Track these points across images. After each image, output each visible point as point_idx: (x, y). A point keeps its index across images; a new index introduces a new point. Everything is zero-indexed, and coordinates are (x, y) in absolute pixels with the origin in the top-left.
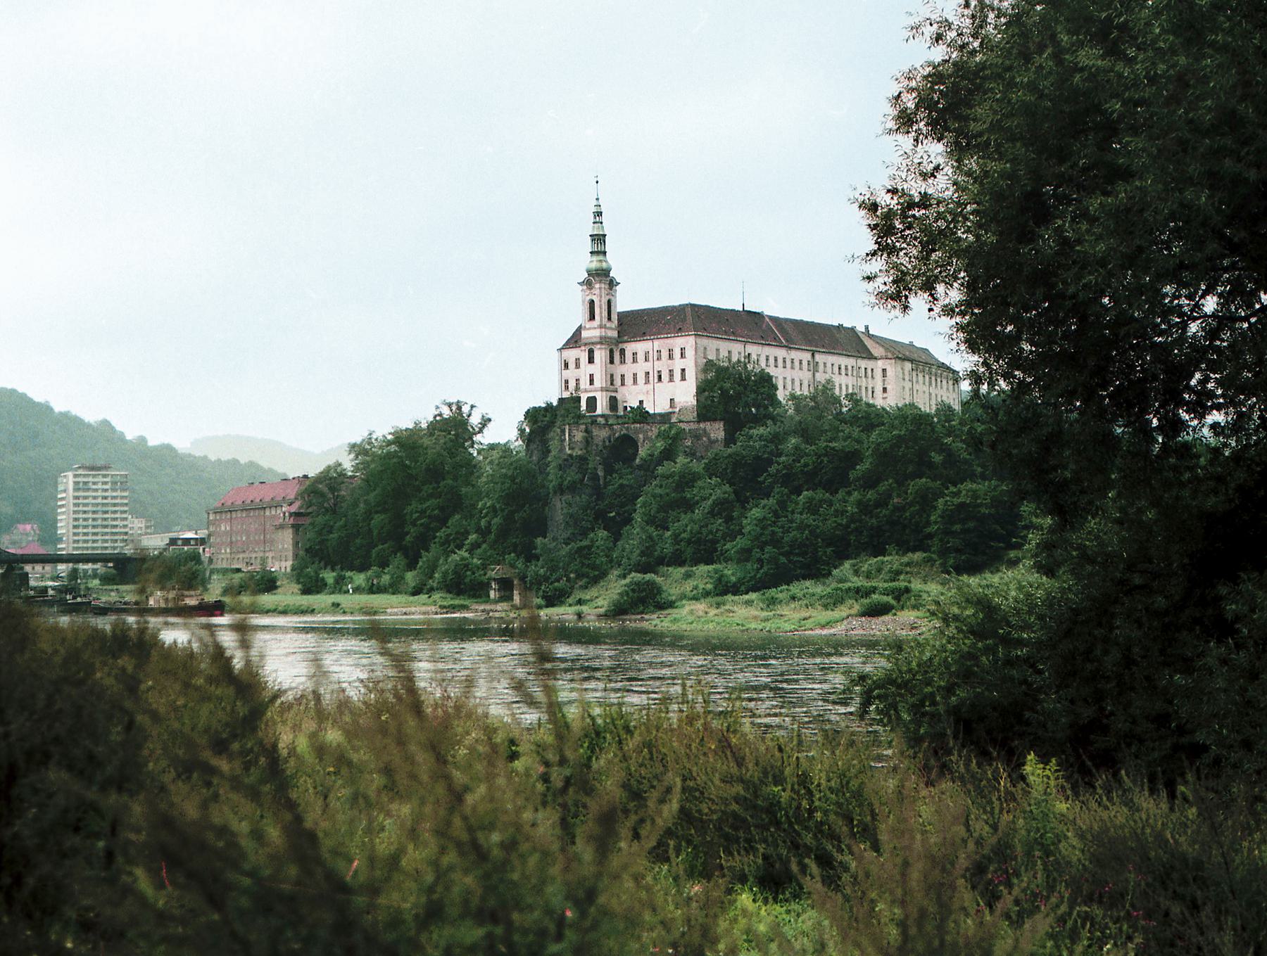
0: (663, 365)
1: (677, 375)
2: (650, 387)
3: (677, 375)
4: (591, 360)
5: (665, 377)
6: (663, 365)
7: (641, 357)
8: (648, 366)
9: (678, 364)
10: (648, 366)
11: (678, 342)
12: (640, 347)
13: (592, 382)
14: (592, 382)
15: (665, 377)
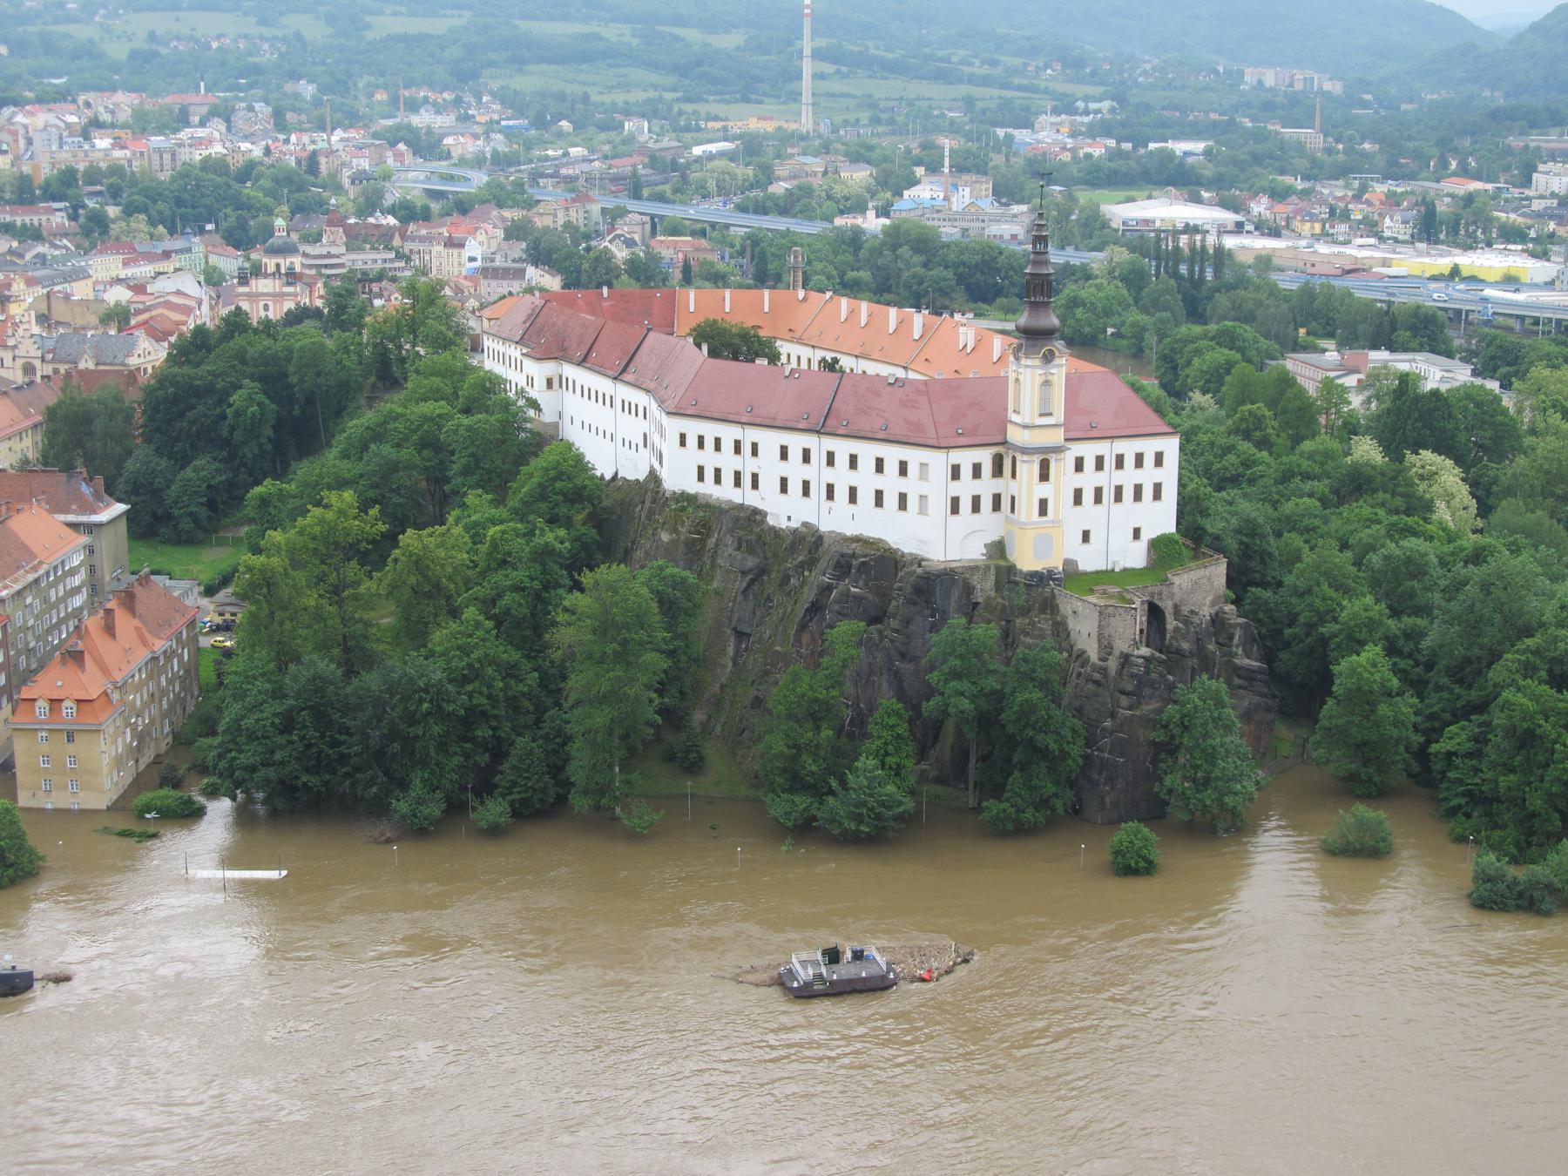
0: (1128, 477)
1: (1148, 492)
2: (1101, 509)
3: (1148, 492)
4: (1044, 476)
5: (1128, 494)
6: (1128, 477)
7: (1089, 464)
8: (1101, 479)
10: (1101, 479)
11: (1149, 447)
12: (1089, 451)
13: (1043, 510)
14: (1043, 510)
15: (1128, 494)
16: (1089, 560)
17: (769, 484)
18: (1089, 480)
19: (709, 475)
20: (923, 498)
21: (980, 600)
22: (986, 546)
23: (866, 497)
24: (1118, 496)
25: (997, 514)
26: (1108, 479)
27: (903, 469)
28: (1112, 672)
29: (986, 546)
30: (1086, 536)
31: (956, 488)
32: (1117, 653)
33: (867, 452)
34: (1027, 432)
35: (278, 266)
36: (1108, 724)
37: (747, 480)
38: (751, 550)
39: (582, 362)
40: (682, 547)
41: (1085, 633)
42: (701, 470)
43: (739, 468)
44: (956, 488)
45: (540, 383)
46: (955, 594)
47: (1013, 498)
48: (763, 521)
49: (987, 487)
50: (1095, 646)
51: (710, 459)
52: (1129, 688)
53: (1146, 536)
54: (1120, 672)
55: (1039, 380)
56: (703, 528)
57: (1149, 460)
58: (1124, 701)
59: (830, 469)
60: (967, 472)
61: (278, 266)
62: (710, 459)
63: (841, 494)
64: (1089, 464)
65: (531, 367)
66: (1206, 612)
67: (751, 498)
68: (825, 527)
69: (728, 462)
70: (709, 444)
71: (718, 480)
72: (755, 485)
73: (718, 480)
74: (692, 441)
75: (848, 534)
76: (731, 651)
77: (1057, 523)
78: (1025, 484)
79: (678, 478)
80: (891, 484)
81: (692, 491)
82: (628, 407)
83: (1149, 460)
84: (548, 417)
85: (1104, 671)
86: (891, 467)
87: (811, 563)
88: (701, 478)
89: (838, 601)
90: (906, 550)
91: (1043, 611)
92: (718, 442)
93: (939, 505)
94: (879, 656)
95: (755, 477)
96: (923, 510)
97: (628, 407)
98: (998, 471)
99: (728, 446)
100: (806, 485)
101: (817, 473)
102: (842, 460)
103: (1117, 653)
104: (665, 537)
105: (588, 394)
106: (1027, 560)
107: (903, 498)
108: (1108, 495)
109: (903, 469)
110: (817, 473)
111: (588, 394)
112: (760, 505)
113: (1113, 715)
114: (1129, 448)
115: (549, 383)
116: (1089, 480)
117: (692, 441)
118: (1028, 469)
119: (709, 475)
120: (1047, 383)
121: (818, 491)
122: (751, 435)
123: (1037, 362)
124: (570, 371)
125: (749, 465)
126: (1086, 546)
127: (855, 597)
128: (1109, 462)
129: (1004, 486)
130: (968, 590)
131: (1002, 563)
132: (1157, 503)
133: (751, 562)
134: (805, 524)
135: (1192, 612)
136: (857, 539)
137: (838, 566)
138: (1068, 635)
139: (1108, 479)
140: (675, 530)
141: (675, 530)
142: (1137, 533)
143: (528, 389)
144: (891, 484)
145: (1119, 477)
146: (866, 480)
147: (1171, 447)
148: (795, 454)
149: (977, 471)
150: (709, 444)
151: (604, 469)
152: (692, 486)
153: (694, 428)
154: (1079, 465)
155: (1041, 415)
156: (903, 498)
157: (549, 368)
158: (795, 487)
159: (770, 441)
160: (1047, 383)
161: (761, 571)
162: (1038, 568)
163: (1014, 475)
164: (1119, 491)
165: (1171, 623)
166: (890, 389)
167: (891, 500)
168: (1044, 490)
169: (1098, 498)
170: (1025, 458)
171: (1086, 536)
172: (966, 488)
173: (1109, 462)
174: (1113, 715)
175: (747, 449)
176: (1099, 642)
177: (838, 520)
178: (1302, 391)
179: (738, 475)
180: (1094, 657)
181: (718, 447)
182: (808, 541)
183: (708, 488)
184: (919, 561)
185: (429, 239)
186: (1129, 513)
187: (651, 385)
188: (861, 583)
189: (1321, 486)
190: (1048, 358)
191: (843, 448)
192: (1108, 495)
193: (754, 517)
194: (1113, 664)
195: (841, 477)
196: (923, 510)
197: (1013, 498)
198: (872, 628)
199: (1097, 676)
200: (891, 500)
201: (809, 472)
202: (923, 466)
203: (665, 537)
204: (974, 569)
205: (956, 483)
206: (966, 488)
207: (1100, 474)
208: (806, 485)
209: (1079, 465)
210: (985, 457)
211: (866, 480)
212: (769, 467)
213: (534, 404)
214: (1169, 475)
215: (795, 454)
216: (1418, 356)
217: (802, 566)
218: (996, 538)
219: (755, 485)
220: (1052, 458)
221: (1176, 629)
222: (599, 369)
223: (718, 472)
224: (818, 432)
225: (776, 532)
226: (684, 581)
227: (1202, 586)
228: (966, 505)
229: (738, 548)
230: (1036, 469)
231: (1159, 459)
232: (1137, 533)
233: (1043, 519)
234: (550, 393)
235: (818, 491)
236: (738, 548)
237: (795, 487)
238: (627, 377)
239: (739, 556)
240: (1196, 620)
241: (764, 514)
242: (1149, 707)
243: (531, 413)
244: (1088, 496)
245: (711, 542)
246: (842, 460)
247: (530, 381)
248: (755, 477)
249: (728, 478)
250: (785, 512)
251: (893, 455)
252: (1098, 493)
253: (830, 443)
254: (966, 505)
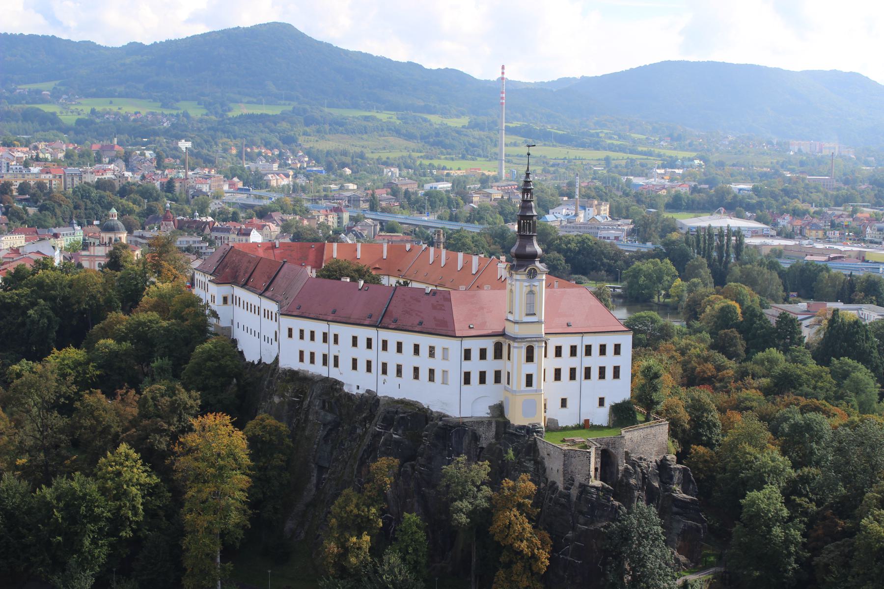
0: (595, 361)
1: (609, 373)
3: (609, 373)
4: (530, 358)
5: (595, 373)
6: (595, 361)
7: (566, 351)
8: (574, 362)
9: (609, 361)
10: (574, 362)
11: (610, 341)
12: (566, 343)
15: (595, 373)
16: (566, 418)
17: (345, 363)
18: (566, 363)
19: (307, 357)
20: (445, 372)
21: (484, 446)
22: (490, 407)
23: (408, 372)
24: (588, 376)
25: (498, 385)
26: (580, 362)
27: (432, 352)
28: (574, 498)
29: (490, 407)
30: (564, 403)
31: (467, 366)
32: (577, 484)
33: (409, 339)
34: (516, 325)
35: (110, 239)
36: (570, 534)
37: (331, 361)
38: (331, 410)
39: (244, 286)
40: (286, 407)
41: (555, 469)
43: (326, 352)
44: (467, 366)
45: (219, 300)
46: (466, 440)
47: (509, 373)
48: (341, 389)
49: (490, 365)
50: (562, 479)
51: (307, 346)
52: (585, 510)
53: (608, 404)
54: (579, 498)
55: (525, 290)
56: (301, 393)
57: (610, 350)
58: (582, 519)
59: (384, 352)
60: (475, 354)
61: (110, 239)
62: (307, 346)
63: (392, 370)
64: (566, 351)
65: (214, 289)
66: (653, 459)
67: (334, 374)
68: (380, 394)
69: (319, 348)
70: (307, 335)
71: (312, 361)
72: (336, 365)
73: (312, 361)
74: (296, 334)
75: (396, 398)
76: (314, 480)
77: (538, 391)
78: (516, 364)
79: (289, 362)
80: (424, 363)
81: (296, 369)
82: (268, 314)
83: (610, 350)
84: (224, 323)
85: (568, 496)
86: (424, 351)
87: (371, 418)
88: (301, 359)
89: (384, 444)
90: (435, 409)
91: (528, 453)
92: (312, 333)
93: (456, 378)
94: (412, 484)
95: (336, 358)
96: (445, 382)
97: (268, 314)
98: (498, 355)
99: (319, 337)
100: (369, 363)
101: (376, 355)
102: (392, 346)
103: (577, 484)
104: (276, 400)
105: (249, 307)
106: (517, 418)
108: (580, 374)
109: (432, 352)
110: (376, 355)
111: (249, 307)
112: (339, 378)
113: (574, 529)
114: (595, 342)
115: (225, 300)
116: (566, 363)
117: (296, 334)
118: (519, 352)
119: (307, 357)
120: (531, 292)
121: (376, 367)
122: (335, 328)
123: (524, 277)
124: (239, 292)
125: (333, 350)
126: (564, 410)
127: (397, 442)
128: (581, 351)
129: (502, 365)
130: (476, 438)
131: (501, 419)
132: (616, 380)
133: (330, 417)
134: (368, 391)
135: (641, 459)
136: (402, 402)
137: (385, 419)
138: (545, 470)
139: (580, 362)
140: (283, 396)
141: (283, 396)
142: (602, 402)
143: (210, 304)
144: (424, 363)
145: (588, 361)
146: (408, 360)
147: (626, 341)
148: (362, 343)
149: (483, 354)
150: (307, 335)
151: (251, 356)
152: (296, 365)
153: (297, 324)
154: (558, 352)
155: (527, 315)
156: (432, 372)
157: (226, 290)
158: (362, 365)
159: (346, 332)
160: (531, 292)
161: (336, 425)
162: (526, 424)
163: (509, 359)
164: (588, 371)
165: (622, 465)
166: (427, 296)
167: (424, 374)
168: (529, 368)
169: (573, 376)
170: (516, 344)
171: (564, 403)
172: (475, 366)
173: (581, 351)
174: (574, 529)
175: (331, 339)
176: (564, 476)
177: (390, 389)
178: (766, 321)
179: (325, 357)
180: (561, 486)
181: (312, 338)
182: (370, 401)
183: (306, 367)
184: (441, 416)
185: (228, 230)
186: (595, 387)
187: (280, 298)
188: (400, 432)
189: (765, 381)
190: (533, 274)
191: (392, 337)
192: (580, 374)
193: (334, 386)
194: (574, 492)
195: (391, 358)
196: (445, 382)
197: (509, 373)
198: (407, 464)
199: (563, 500)
200: (424, 374)
201: (384, 357)
202: (445, 350)
203: (276, 400)
204: (480, 422)
205: (467, 362)
206: (475, 366)
207: (573, 358)
208: (369, 363)
209: (558, 352)
210: (489, 344)
211: (408, 360)
212: (345, 351)
213: (215, 314)
214: (625, 361)
215: (362, 343)
216: (863, 306)
217: (365, 419)
218: (497, 402)
219: (336, 365)
220: (536, 345)
221: (626, 469)
222: (253, 290)
223: (312, 355)
224: (377, 327)
225: (349, 396)
226: (277, 429)
227: (650, 442)
228: (475, 378)
229: (323, 408)
230: (524, 352)
231: (617, 349)
232: (602, 402)
233: (529, 388)
234: (225, 307)
235: (376, 367)
236: (323, 408)
237: (362, 365)
238: (268, 294)
239: (323, 413)
240: (644, 464)
241: (341, 384)
242: (601, 525)
243: (213, 321)
244: (565, 374)
245: (306, 403)
246: (392, 346)
247: (213, 298)
248: (336, 358)
249: (319, 359)
250: (356, 383)
251: (425, 341)
252: (573, 372)
253: (384, 334)
254: (475, 378)
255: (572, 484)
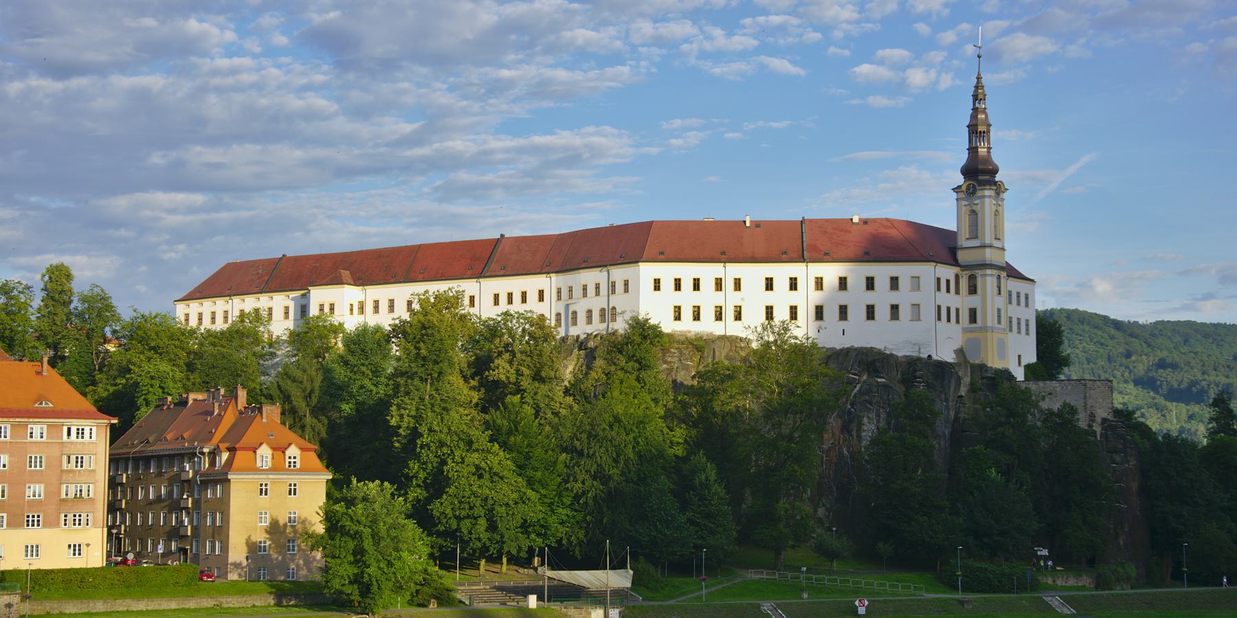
42: (678, 310)
43: (721, 303)
72: (738, 317)
75: (838, 347)
103: (1099, 420)
107: (895, 308)
109: (894, 283)
125: (730, 299)
144: (882, 298)
156: (895, 308)
159: (753, 274)
167: (882, 312)
181: (696, 285)
194: (1097, 428)
200: (882, 312)
255: (1093, 421)
